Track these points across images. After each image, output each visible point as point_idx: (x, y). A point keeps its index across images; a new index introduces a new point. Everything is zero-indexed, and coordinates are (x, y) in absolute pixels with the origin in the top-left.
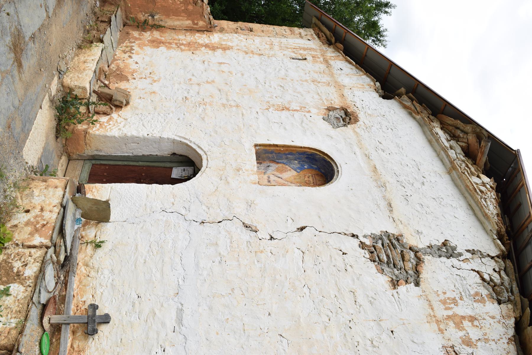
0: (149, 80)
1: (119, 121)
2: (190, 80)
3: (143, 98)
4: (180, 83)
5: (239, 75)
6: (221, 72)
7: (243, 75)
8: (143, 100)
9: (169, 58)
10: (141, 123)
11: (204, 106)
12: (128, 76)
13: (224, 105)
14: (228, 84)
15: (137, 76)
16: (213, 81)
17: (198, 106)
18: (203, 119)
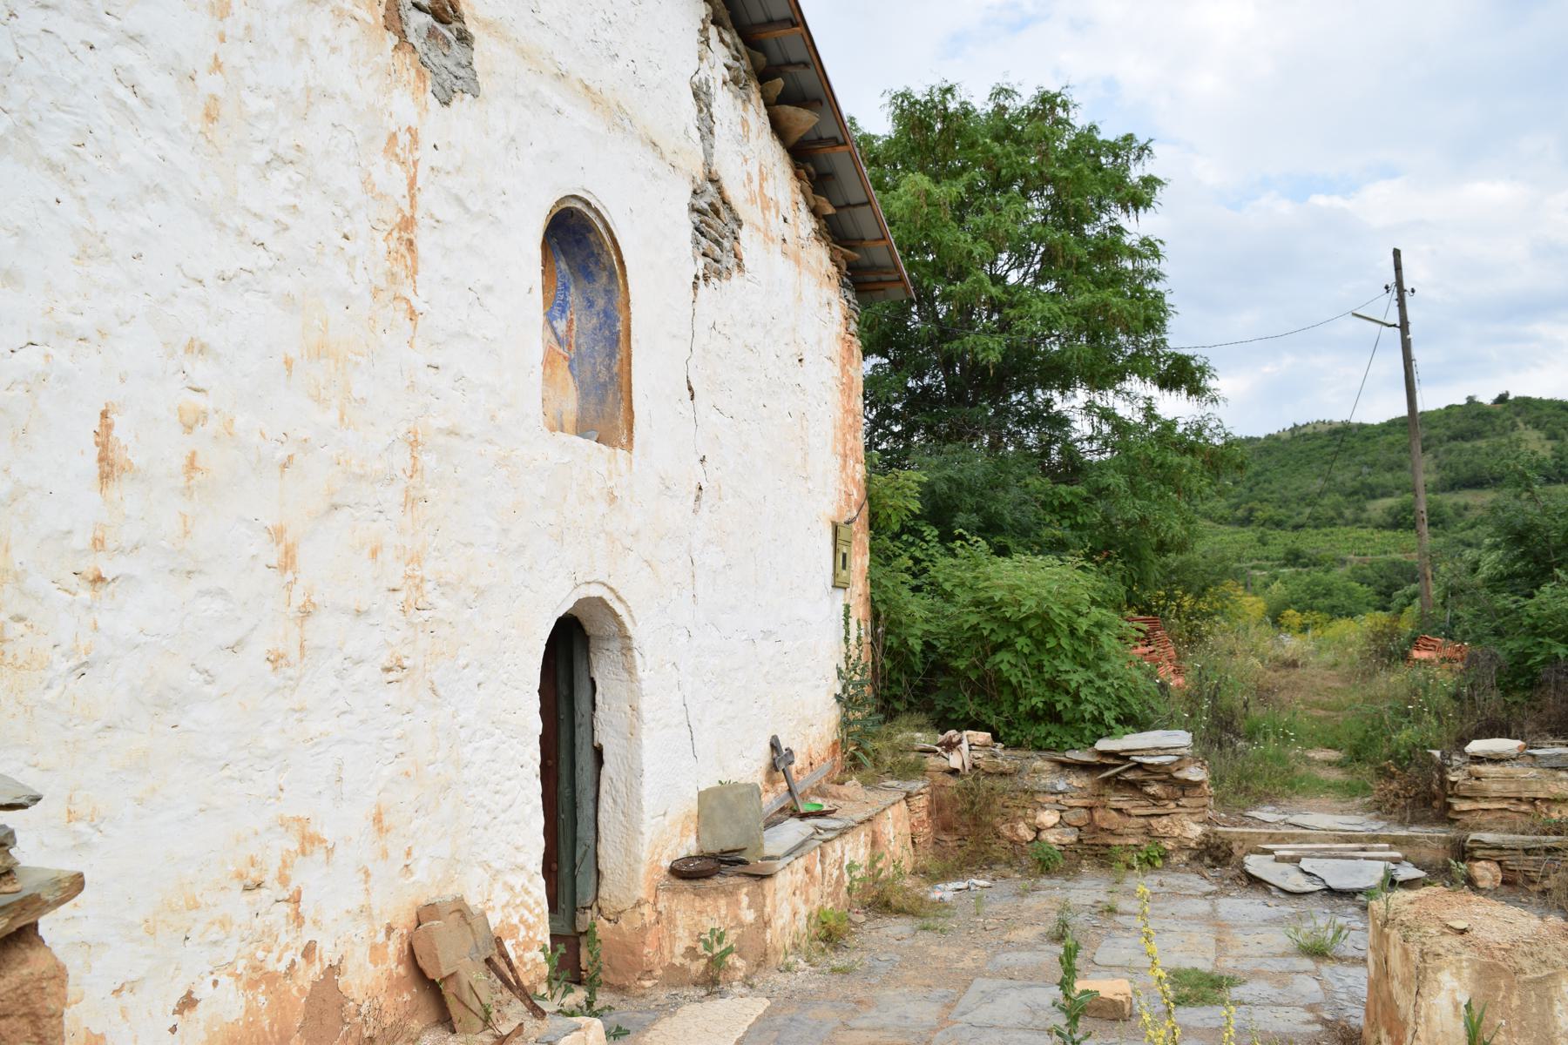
0: (309, 877)
1: (506, 896)
2: (276, 660)
3: (409, 854)
4: (301, 710)
5: (200, 370)
6: (198, 476)
7: (197, 348)
8: (415, 854)
9: (80, 826)
10: (502, 817)
11: (428, 587)
12: (301, 990)
13: (410, 502)
14: (290, 457)
15: (287, 947)
16: (277, 534)
17: (426, 614)
18: (480, 592)
